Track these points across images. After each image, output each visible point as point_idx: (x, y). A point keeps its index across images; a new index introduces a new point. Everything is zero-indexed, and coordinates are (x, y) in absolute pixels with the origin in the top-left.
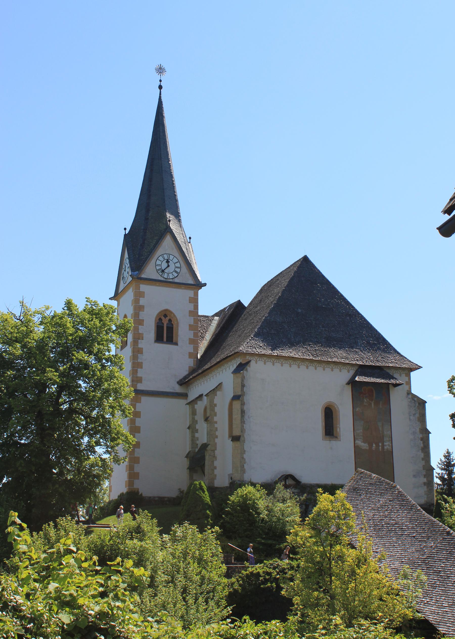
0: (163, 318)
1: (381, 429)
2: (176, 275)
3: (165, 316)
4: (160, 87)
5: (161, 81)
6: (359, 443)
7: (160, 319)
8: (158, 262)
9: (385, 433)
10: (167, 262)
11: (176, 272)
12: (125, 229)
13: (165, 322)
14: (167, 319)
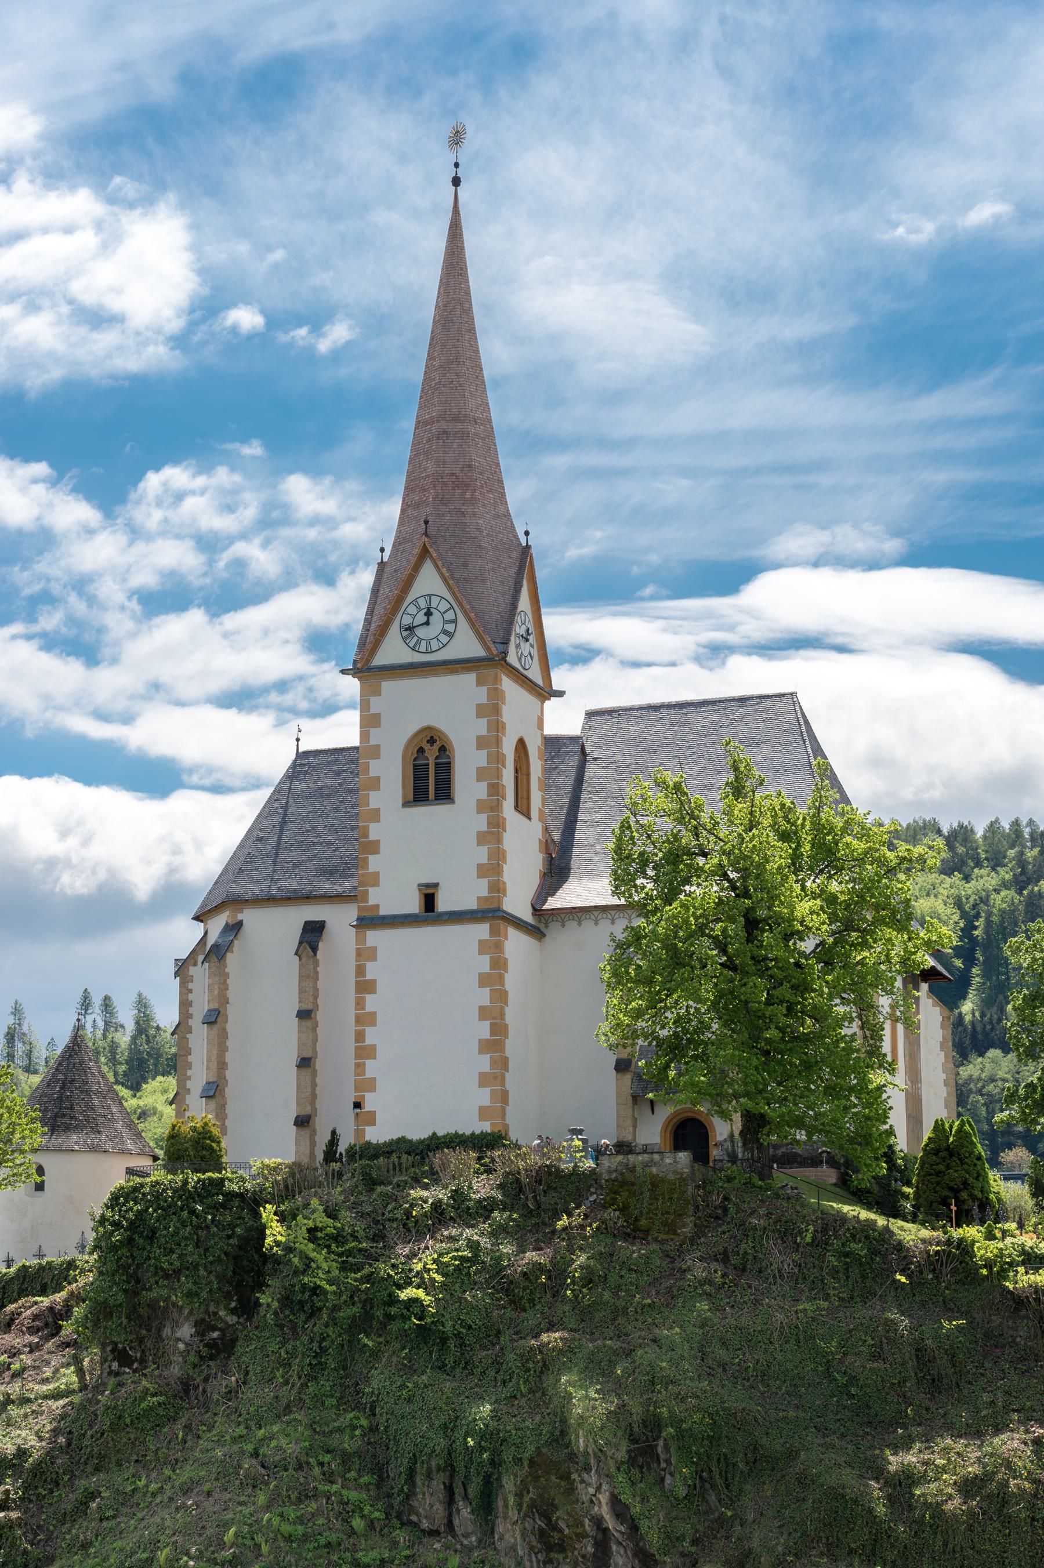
0: (427, 747)
3: (432, 741)
4: (456, 182)
5: (457, 165)
7: (421, 750)
10: (425, 614)
11: (445, 632)
12: (382, 550)
13: (431, 754)
14: (436, 747)
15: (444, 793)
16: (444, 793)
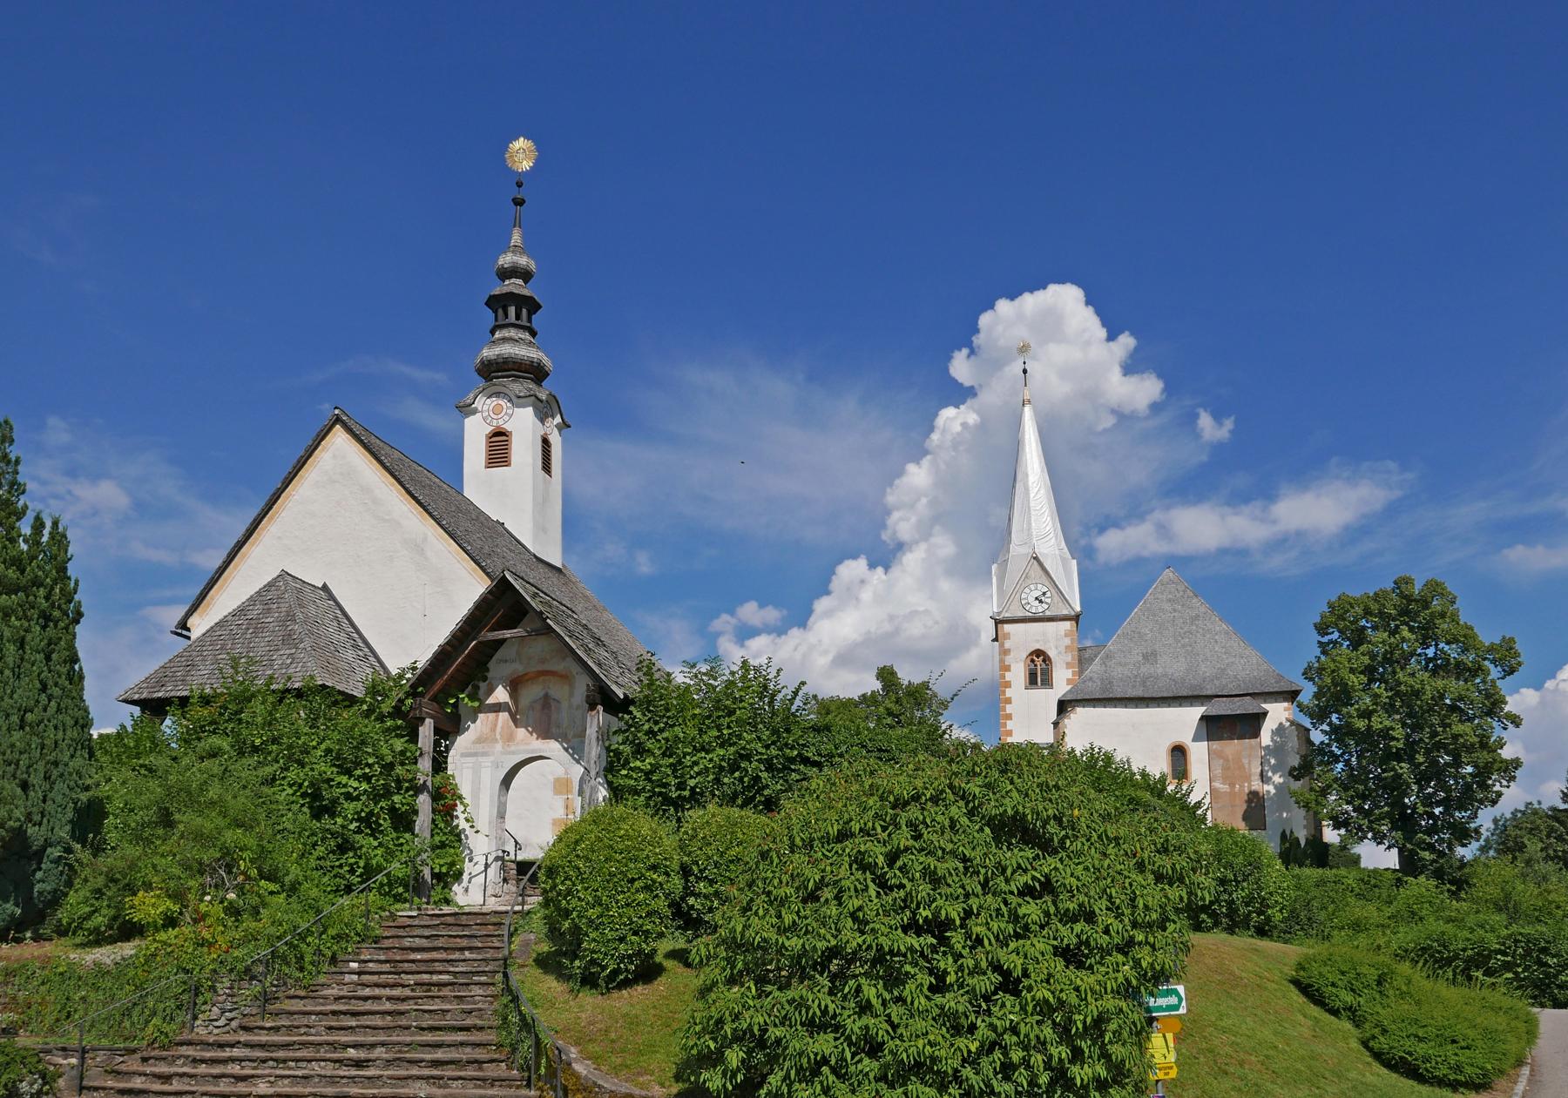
1: (1247, 766)
2: (1046, 606)
6: (1217, 785)
7: (1033, 661)
8: (1024, 596)
9: (1253, 770)
13: (1039, 661)
15: (1047, 682)
16: (1047, 682)
